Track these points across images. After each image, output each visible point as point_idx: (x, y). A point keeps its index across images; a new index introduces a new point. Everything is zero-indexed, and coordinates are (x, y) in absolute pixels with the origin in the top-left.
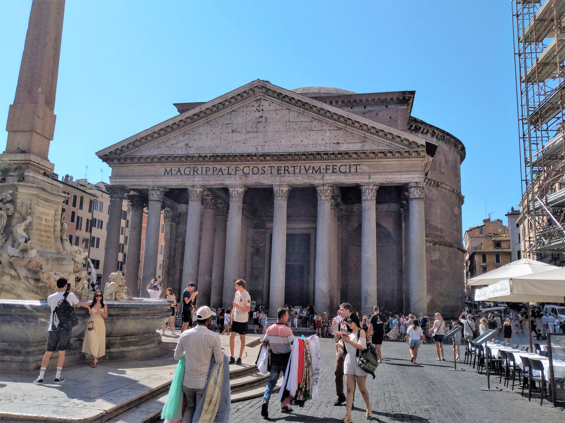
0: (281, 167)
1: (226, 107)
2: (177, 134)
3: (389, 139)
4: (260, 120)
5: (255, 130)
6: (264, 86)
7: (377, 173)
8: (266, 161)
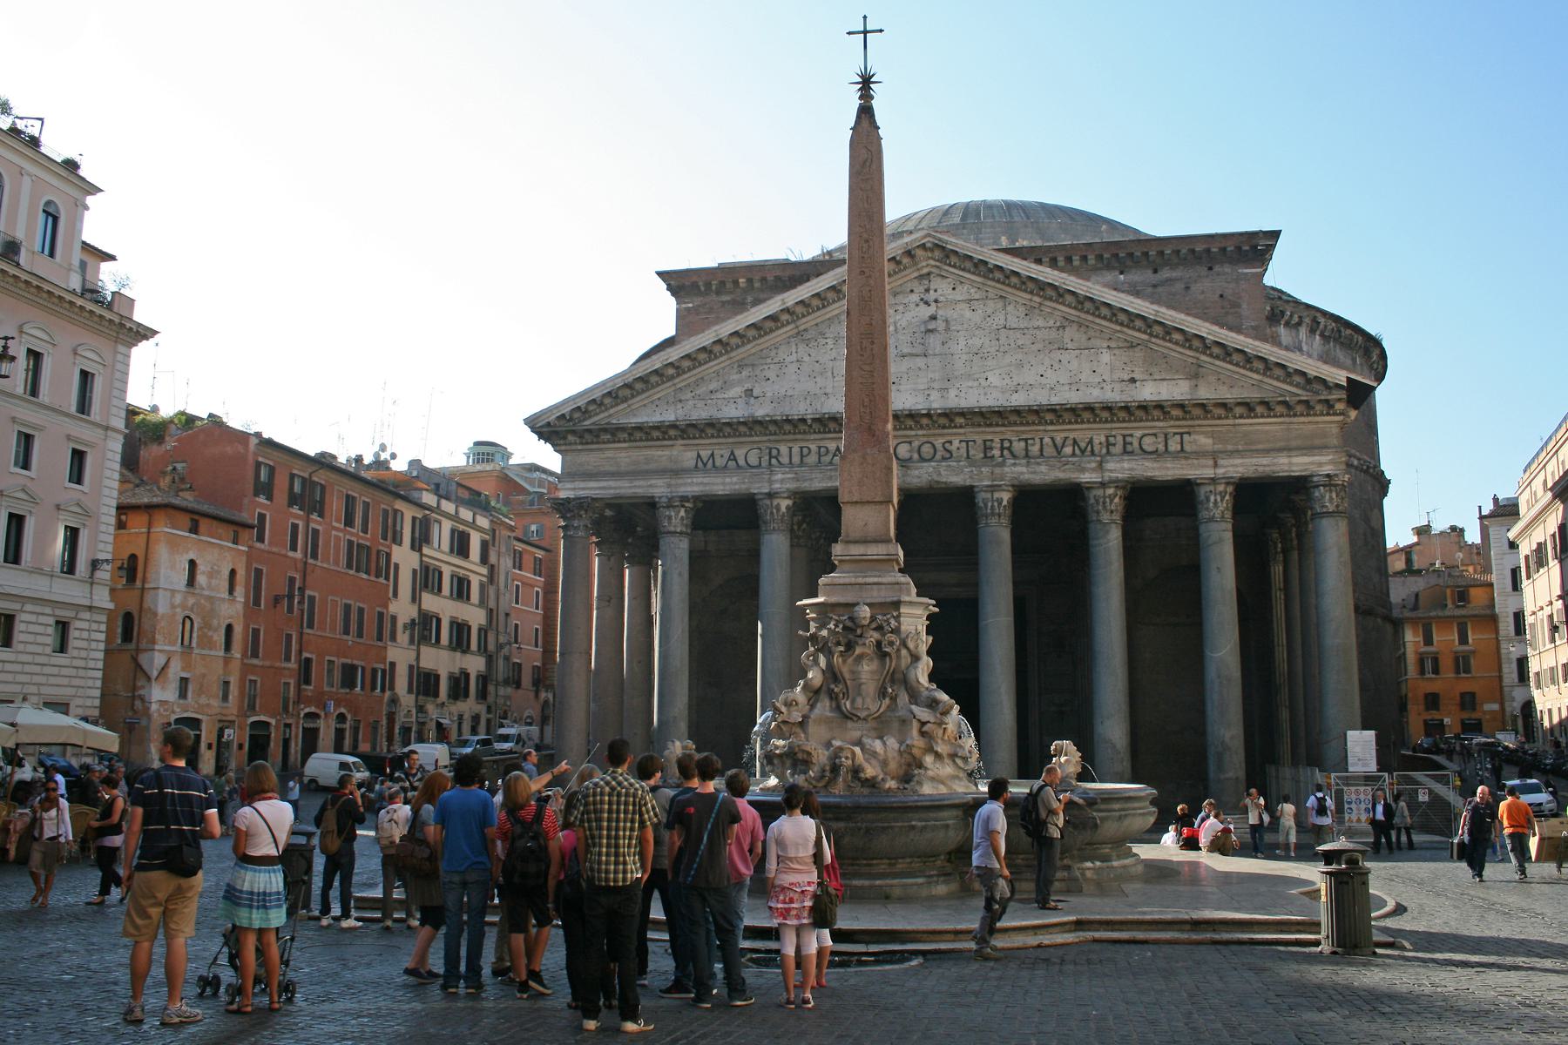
0: (992, 440)
2: (722, 365)
3: (1257, 372)
4: (932, 326)
5: (918, 349)
6: (940, 243)
7: (1232, 452)
8: (955, 427)
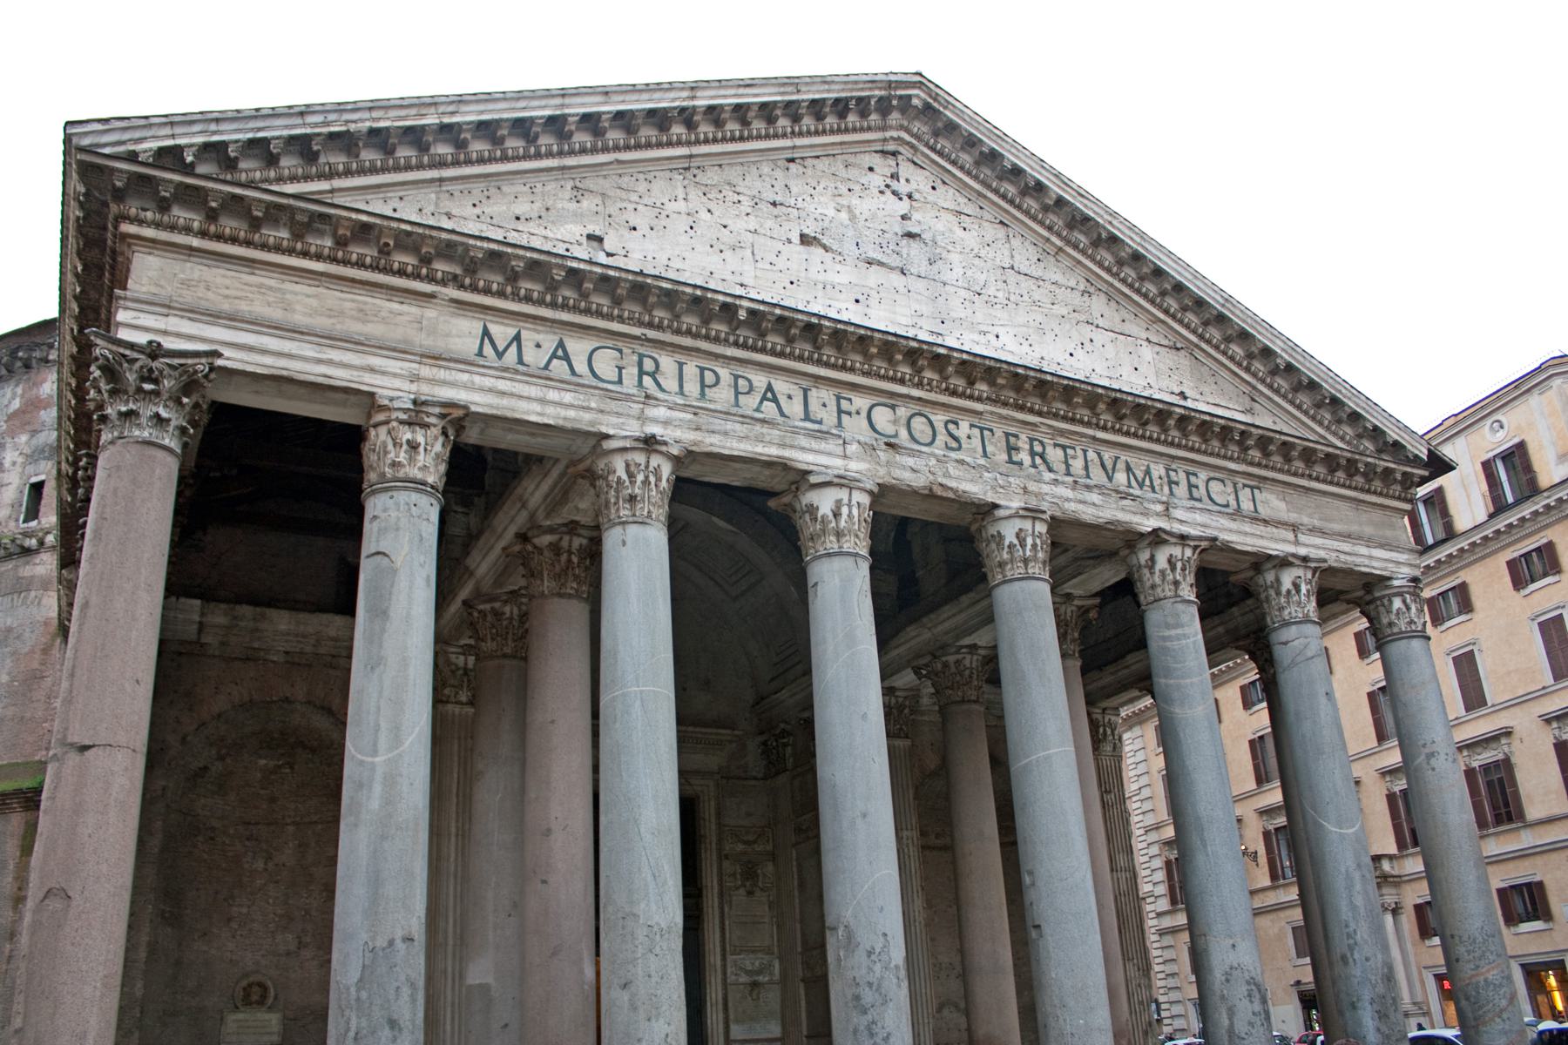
0: (1016, 436)
1: (776, 136)
3: (1320, 424)
5: (894, 261)
6: (936, 105)
8: (971, 397)
